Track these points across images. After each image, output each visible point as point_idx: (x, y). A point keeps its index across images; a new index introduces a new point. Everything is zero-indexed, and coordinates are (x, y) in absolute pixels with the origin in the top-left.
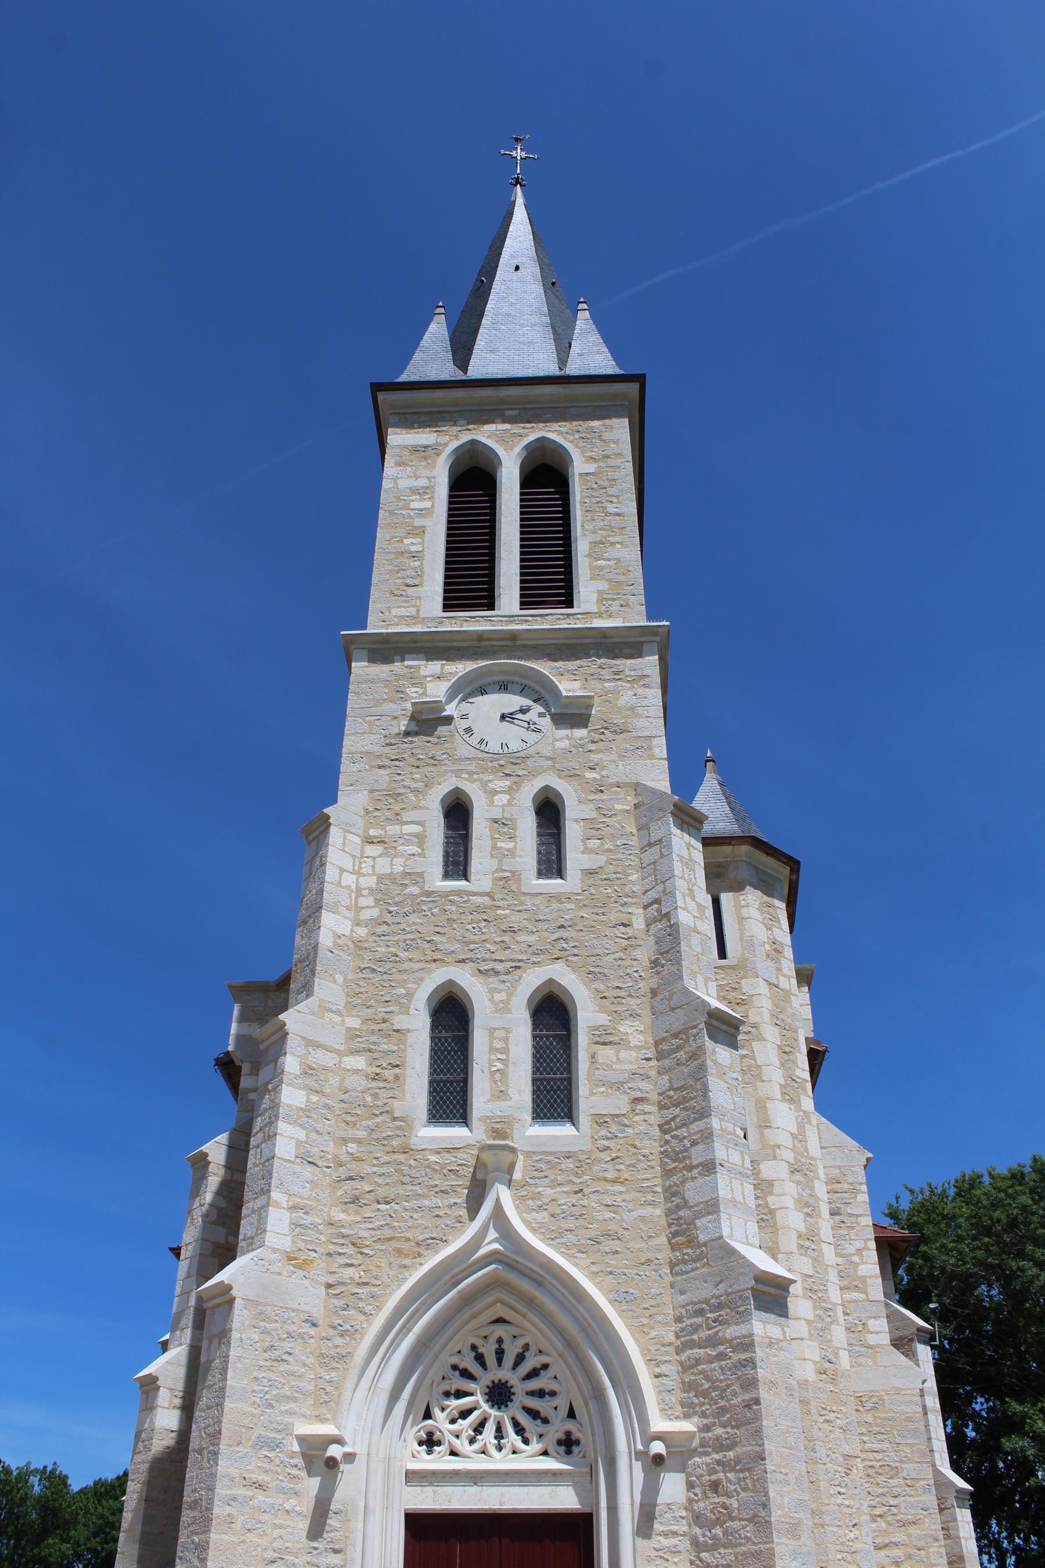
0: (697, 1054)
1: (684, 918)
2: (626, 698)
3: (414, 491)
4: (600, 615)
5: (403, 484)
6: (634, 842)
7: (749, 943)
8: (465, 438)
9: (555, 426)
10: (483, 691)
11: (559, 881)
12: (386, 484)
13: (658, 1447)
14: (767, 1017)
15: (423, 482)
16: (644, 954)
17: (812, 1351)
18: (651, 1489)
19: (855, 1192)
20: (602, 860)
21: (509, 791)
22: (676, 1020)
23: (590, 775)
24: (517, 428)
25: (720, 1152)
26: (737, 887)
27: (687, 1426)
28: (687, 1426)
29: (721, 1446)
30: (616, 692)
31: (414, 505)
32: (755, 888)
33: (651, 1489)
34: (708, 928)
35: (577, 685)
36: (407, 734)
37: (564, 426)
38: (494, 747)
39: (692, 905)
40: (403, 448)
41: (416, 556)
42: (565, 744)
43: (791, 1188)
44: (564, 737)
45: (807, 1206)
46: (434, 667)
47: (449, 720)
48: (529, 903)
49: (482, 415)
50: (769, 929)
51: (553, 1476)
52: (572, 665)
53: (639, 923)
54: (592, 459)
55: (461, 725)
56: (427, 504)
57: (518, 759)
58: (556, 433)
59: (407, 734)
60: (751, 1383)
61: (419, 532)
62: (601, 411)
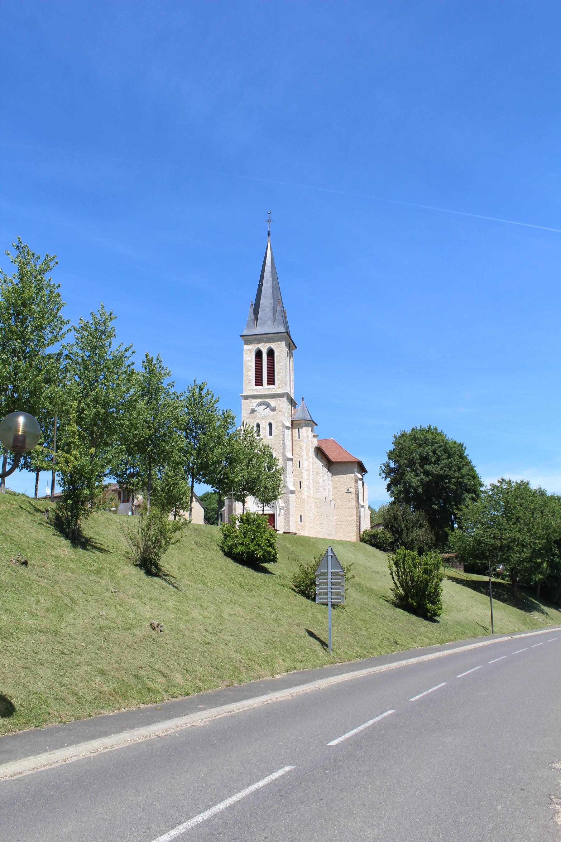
0: (286, 463)
1: (286, 444)
2: (281, 405)
3: (249, 361)
4: (278, 388)
5: (248, 359)
6: (281, 431)
7: (303, 437)
8: (257, 347)
9: (272, 344)
10: (261, 405)
11: (271, 437)
12: (244, 359)
13: (281, 507)
14: (304, 448)
15: (250, 359)
16: (282, 448)
17: (306, 494)
18: (280, 511)
19: (320, 470)
20: (277, 433)
21: (265, 422)
22: (285, 458)
23: (276, 419)
24: (266, 344)
25: (288, 475)
26: (302, 428)
27: (284, 505)
28: (284, 505)
29: (287, 507)
30: (280, 404)
31: (249, 364)
32: (305, 426)
33: (280, 511)
34: (290, 444)
35: (274, 403)
36: (250, 413)
37: (273, 344)
38: (263, 415)
39: (288, 441)
40: (246, 349)
41: (250, 376)
42: (272, 414)
43: (306, 473)
44: (272, 413)
45: (308, 475)
46: (254, 400)
47: (256, 411)
48: (267, 441)
49: (259, 342)
50: (307, 433)
51: (271, 510)
52: (274, 399)
53: (282, 443)
54: (278, 352)
55: (258, 411)
56: (251, 364)
57: (266, 417)
58: (273, 345)
59: (250, 413)
60: (289, 501)
61: (250, 370)
62: (280, 340)
